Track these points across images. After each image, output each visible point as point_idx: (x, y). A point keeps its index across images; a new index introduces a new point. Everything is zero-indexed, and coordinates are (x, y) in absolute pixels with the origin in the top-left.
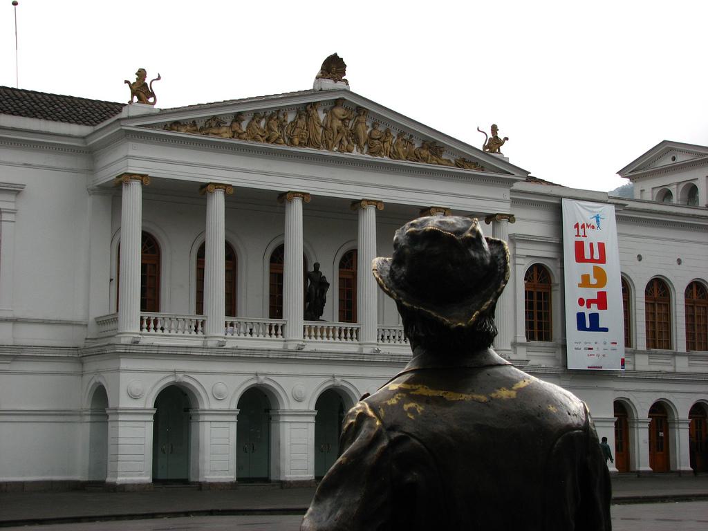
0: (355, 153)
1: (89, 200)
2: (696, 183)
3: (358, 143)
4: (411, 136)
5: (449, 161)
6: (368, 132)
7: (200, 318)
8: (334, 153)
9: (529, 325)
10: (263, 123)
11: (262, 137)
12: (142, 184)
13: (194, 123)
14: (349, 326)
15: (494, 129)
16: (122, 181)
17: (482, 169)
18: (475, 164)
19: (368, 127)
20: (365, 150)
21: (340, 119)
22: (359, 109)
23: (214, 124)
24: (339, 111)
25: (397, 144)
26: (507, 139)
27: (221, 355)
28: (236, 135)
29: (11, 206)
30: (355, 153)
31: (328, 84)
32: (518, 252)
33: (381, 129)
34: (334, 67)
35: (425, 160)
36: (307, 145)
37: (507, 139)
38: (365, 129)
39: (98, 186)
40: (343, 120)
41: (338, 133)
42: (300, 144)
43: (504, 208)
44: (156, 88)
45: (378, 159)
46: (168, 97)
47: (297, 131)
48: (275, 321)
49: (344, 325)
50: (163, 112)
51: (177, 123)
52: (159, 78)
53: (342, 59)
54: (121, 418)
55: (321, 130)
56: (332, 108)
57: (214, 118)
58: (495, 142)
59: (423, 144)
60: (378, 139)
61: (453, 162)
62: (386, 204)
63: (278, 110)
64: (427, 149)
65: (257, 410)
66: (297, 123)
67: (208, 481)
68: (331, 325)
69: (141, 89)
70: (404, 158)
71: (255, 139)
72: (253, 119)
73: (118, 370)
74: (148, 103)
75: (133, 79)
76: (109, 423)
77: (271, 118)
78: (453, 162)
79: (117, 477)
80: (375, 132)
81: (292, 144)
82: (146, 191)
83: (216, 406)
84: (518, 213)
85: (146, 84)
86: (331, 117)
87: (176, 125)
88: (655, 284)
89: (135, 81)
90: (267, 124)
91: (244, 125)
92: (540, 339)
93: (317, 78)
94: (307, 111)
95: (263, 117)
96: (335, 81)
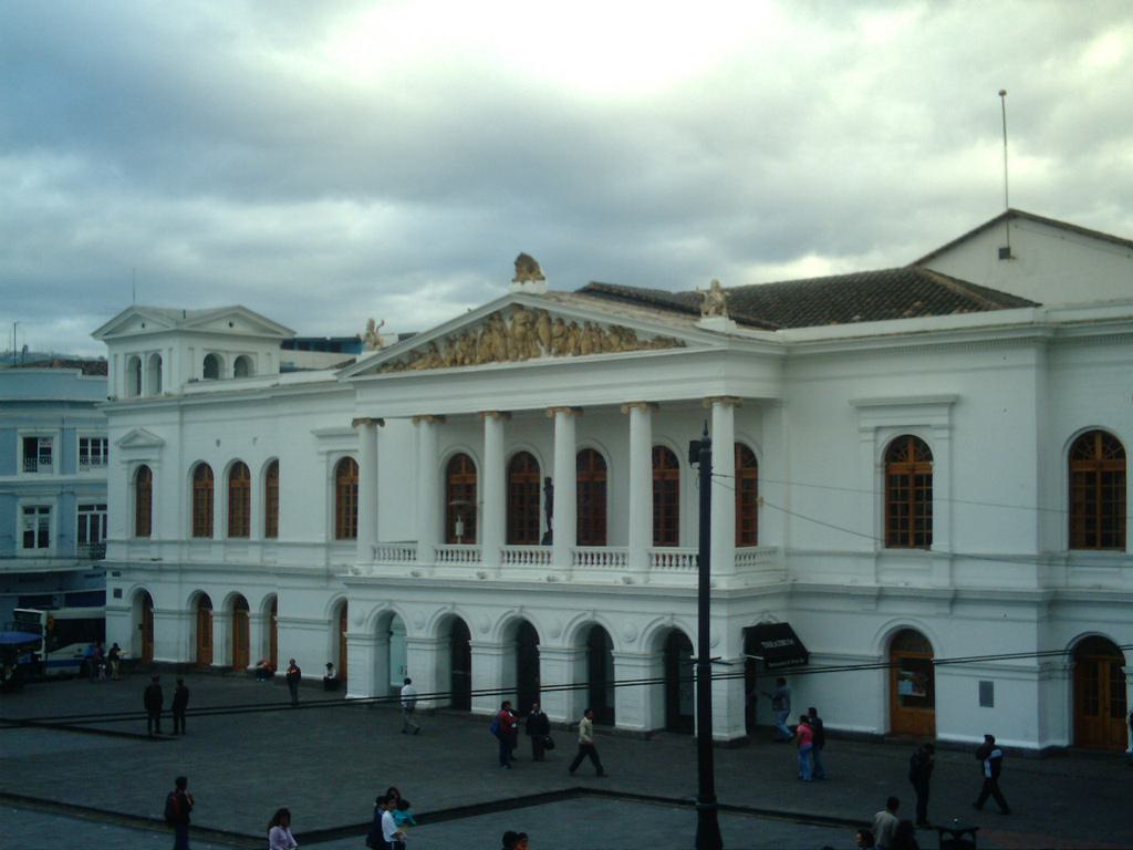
8: (506, 365)
13: (399, 362)
17: (683, 345)
23: (416, 356)
24: (519, 316)
30: (546, 359)
31: (518, 287)
33: (568, 323)
40: (524, 324)
42: (483, 362)
45: (562, 360)
78: (650, 341)
96: (523, 282)
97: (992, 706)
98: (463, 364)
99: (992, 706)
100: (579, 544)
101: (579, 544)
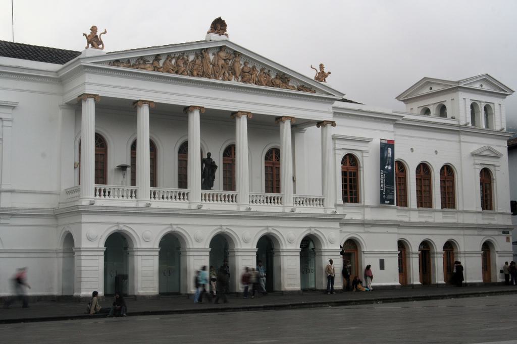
0: (234, 82)
1: (60, 113)
2: (445, 103)
3: (234, 73)
4: (269, 71)
5: (293, 87)
6: (241, 67)
7: (134, 188)
9: (345, 193)
10: (173, 61)
11: (173, 70)
12: (95, 100)
13: (128, 61)
14: (231, 193)
15: (321, 66)
16: (83, 97)
17: (315, 92)
18: (309, 89)
19: (241, 64)
20: (240, 79)
21: (223, 59)
22: (235, 52)
23: (142, 62)
24: (222, 54)
25: (261, 76)
26: (330, 73)
27: (148, 213)
28: (156, 69)
29: (9, 117)
30: (234, 82)
31: (215, 37)
32: (337, 146)
33: (250, 66)
34: (219, 26)
35: (278, 86)
36: (202, 76)
37: (330, 73)
38: (240, 65)
39: (66, 103)
40: (225, 60)
41: (222, 67)
42: (198, 75)
43: (329, 117)
44: (103, 38)
45: (248, 85)
46: (112, 44)
47: (196, 67)
48: (182, 190)
49: (270, 195)
50: (109, 54)
51: (117, 61)
52: (105, 32)
53: (224, 21)
54: (83, 253)
55: (211, 66)
56: (218, 52)
57: (142, 58)
58: (322, 75)
59: (277, 75)
60: (248, 72)
61: (296, 87)
62: (253, 114)
63: (183, 53)
64: (279, 79)
65: (172, 248)
66: (195, 61)
67: (141, 294)
68: (219, 193)
69: (94, 40)
70: (265, 85)
71: (168, 72)
72: (167, 59)
73: (80, 223)
74: (98, 48)
75: (89, 33)
76: (75, 257)
77: (178, 58)
79: (81, 292)
80: (245, 68)
81: (192, 75)
82: (98, 107)
83: (145, 245)
84: (338, 121)
85: (97, 36)
86: (217, 58)
87: (116, 62)
88: (422, 166)
89: (90, 34)
90: (176, 62)
91: (161, 63)
92: (352, 202)
93: (208, 33)
94: (202, 54)
95: (174, 58)
96: (220, 35)
97: (384, 269)
98: (181, 74)
99: (384, 269)
100: (267, 191)
101: (267, 191)
